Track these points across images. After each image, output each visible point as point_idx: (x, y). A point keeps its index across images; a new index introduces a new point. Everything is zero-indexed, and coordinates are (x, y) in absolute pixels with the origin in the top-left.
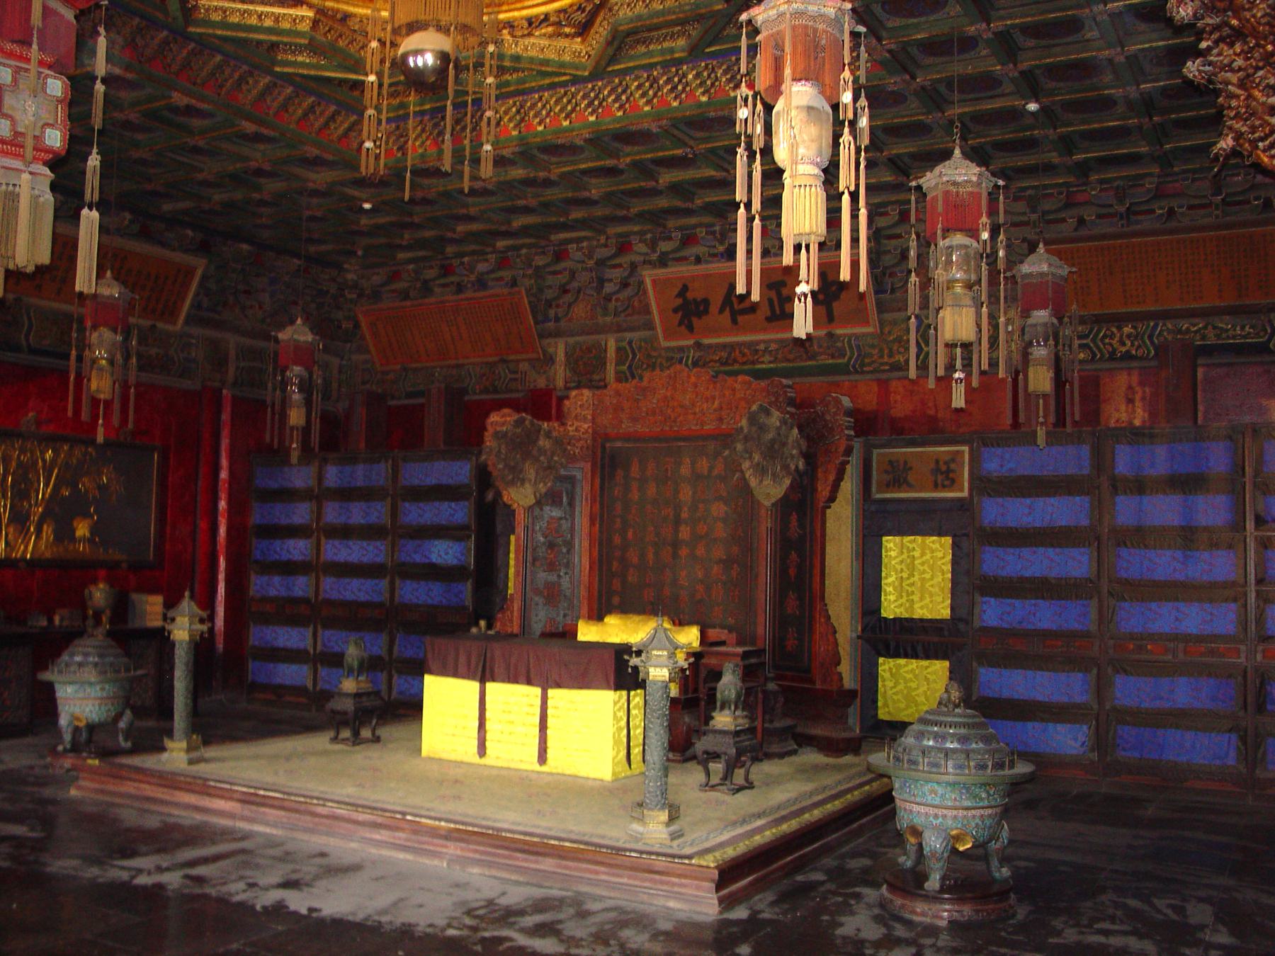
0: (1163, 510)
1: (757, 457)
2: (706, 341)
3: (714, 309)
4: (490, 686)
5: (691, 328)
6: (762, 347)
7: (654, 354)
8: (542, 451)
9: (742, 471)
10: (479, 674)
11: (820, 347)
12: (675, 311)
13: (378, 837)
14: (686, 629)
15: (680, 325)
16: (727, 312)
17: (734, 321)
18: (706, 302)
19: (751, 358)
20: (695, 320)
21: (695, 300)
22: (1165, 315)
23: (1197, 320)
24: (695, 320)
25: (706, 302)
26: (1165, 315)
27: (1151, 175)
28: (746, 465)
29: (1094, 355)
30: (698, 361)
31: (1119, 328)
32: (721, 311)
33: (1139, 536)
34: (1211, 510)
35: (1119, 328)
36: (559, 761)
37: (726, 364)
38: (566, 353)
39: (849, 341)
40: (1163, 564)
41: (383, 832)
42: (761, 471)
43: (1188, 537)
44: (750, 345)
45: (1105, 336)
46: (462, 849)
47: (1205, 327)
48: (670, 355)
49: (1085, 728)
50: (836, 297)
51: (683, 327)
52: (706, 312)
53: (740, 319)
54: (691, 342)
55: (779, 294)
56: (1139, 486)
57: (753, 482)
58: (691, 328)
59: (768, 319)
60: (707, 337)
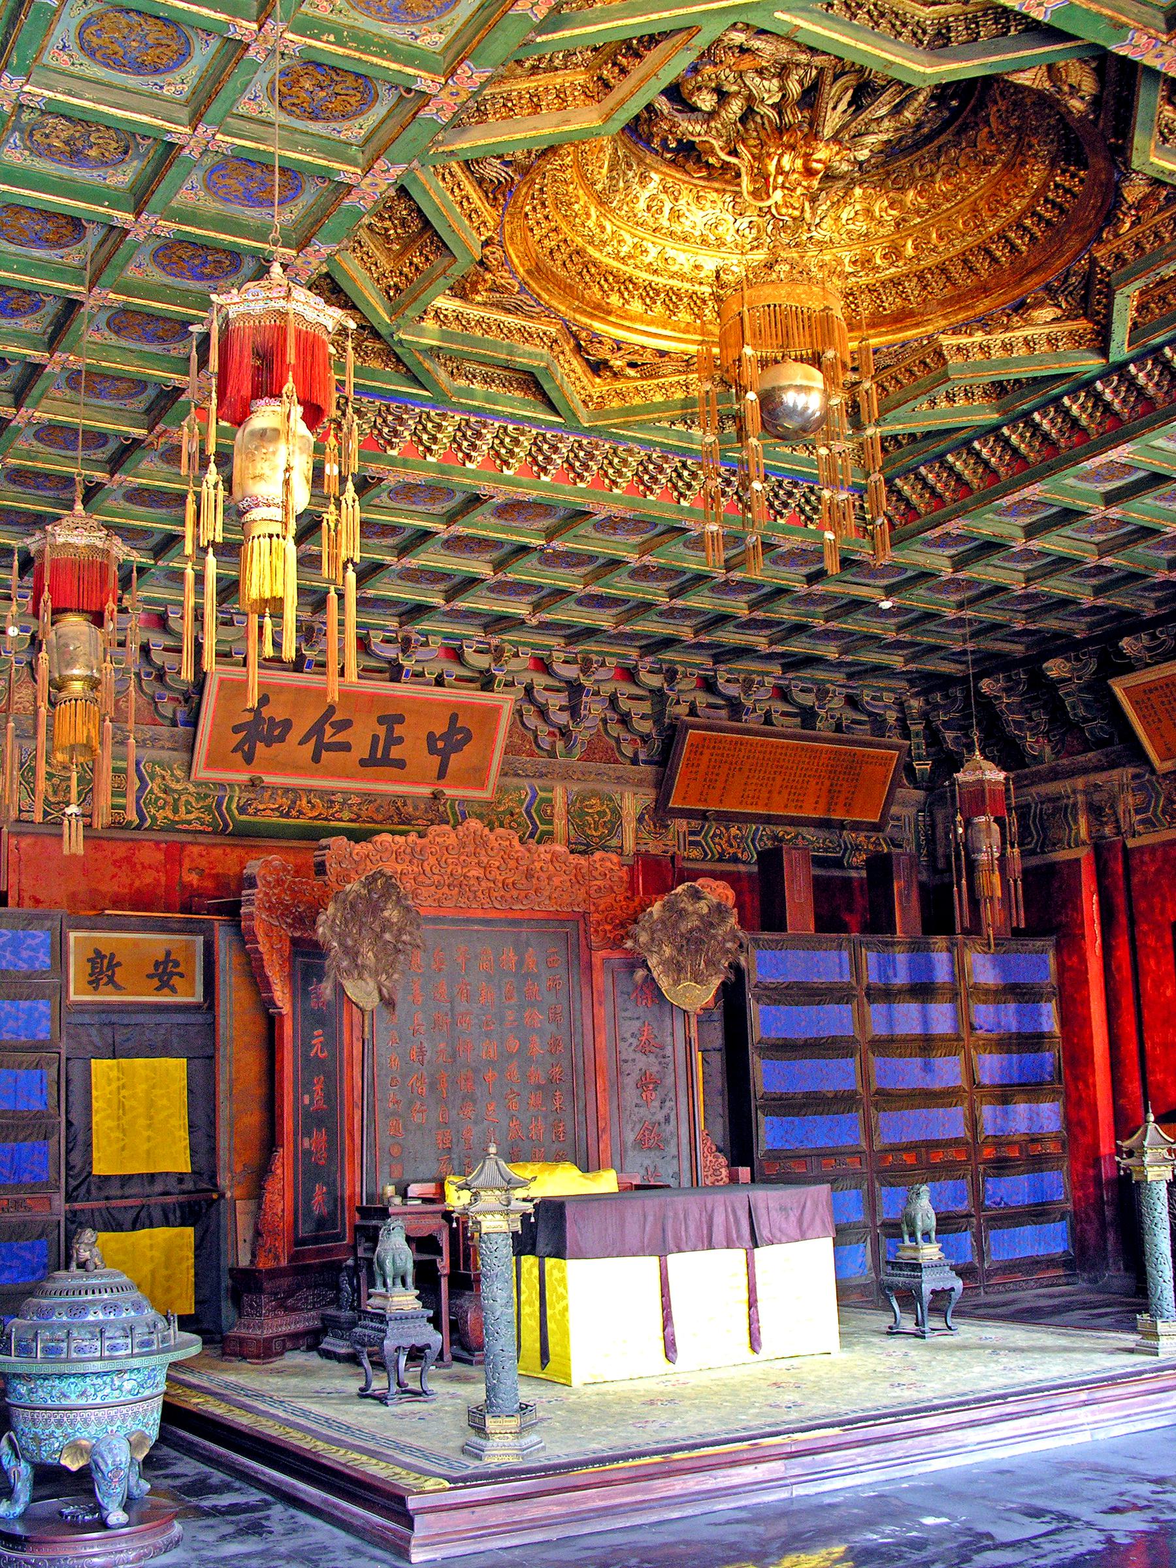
0: (907, 1018)
1: (667, 951)
2: (267, 779)
3: (294, 736)
4: (673, 1259)
5: (249, 759)
6: (339, 798)
7: (179, 787)
8: (386, 926)
9: (649, 970)
11: (416, 808)
12: (236, 729)
15: (234, 751)
16: (311, 745)
17: (316, 758)
18: (287, 725)
19: (325, 812)
20: (260, 746)
21: (272, 719)
22: (768, 820)
23: (788, 828)
24: (260, 746)
25: (287, 725)
26: (768, 820)
27: (768, 674)
28: (652, 961)
29: (706, 854)
30: (248, 803)
31: (727, 829)
33: (886, 1045)
34: (941, 1018)
35: (727, 829)
38: (22, 765)
39: (452, 807)
40: (909, 1073)
42: (676, 968)
43: (926, 1044)
44: (323, 793)
45: (715, 835)
46: (1093, 1413)
47: (796, 837)
48: (203, 790)
50: (458, 747)
51: (239, 754)
52: (281, 739)
54: (245, 777)
55: (390, 730)
56: (886, 994)
57: (664, 983)
58: (249, 759)
59: (363, 763)
60: (268, 773)
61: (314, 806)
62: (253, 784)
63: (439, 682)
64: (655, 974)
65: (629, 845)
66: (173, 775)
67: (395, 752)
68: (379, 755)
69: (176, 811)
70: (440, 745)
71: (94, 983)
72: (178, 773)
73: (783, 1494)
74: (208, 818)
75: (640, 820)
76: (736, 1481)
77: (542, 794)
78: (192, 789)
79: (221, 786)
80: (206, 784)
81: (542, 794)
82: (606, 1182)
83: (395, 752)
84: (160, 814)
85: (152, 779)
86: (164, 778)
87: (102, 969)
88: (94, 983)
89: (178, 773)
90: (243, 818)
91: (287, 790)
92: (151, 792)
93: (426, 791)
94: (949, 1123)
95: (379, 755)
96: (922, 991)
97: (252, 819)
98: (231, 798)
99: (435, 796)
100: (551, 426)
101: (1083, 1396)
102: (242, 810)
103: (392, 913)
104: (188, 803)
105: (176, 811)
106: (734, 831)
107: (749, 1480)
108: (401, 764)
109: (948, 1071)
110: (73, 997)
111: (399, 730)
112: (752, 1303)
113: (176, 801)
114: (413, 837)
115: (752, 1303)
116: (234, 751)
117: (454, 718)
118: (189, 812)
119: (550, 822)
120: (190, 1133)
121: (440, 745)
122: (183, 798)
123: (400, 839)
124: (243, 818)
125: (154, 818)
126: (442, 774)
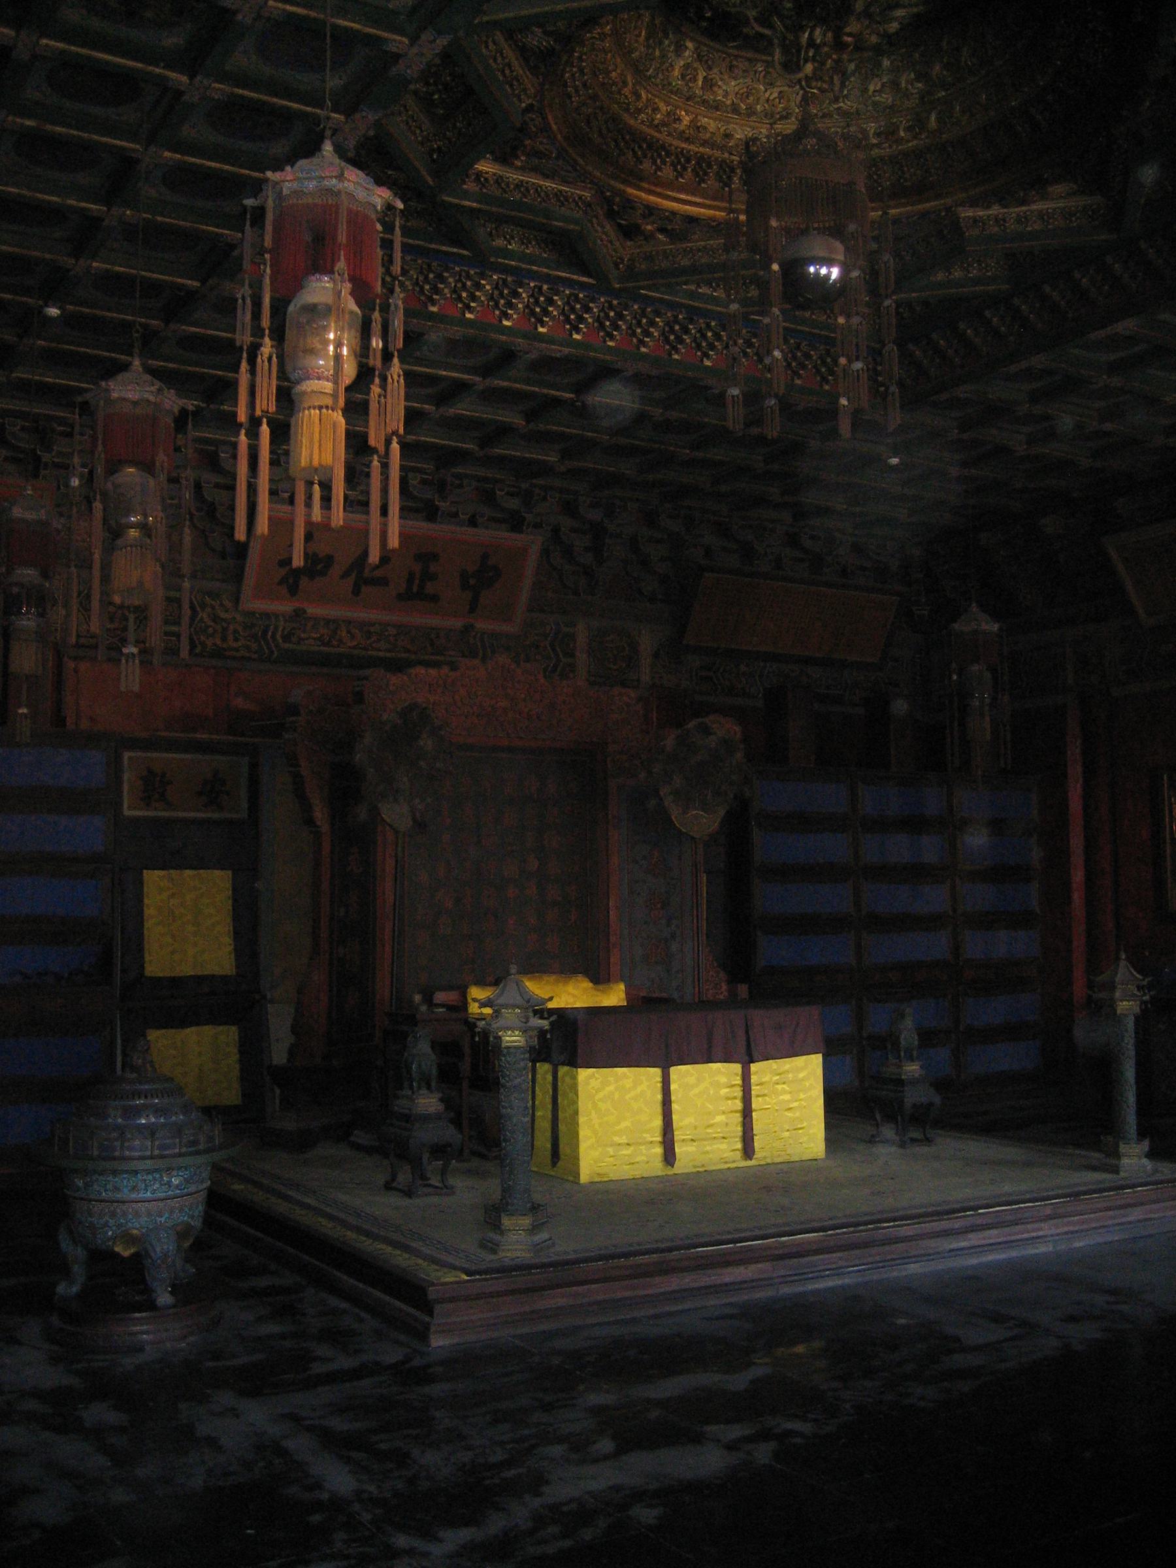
0: (898, 848)
2: (311, 610)
3: (336, 570)
4: (676, 1072)
5: (293, 590)
10: (743, 1050)
13: (963, 1244)
14: (614, 986)
15: (280, 583)
16: (351, 579)
17: (356, 591)
28: (664, 791)
32: (345, 575)
36: (767, 1149)
37: (328, 644)
41: (970, 1236)
43: (917, 873)
49: (848, 1058)
53: (364, 589)
54: (285, 607)
57: (675, 813)
58: (293, 590)
59: (400, 597)
61: (353, 637)
62: (298, 614)
63: (472, 522)
64: (666, 804)
65: (646, 678)
66: (222, 605)
67: (430, 588)
68: (415, 589)
69: (224, 639)
70: (472, 582)
71: (147, 799)
72: (227, 603)
73: (769, 1293)
74: (254, 646)
75: (656, 655)
76: (727, 1280)
77: (566, 630)
78: (239, 618)
79: (267, 615)
80: (253, 613)
81: (566, 630)
82: (615, 997)
83: (430, 588)
84: (209, 642)
85: (203, 609)
86: (213, 608)
87: (154, 786)
88: (147, 799)
89: (227, 603)
90: (287, 646)
91: (328, 622)
92: (202, 619)
93: (458, 624)
94: (932, 946)
95: (415, 589)
96: (914, 824)
97: (295, 646)
98: (276, 628)
99: (467, 629)
100: (583, 286)
101: (1048, 1211)
102: (286, 638)
103: (427, 743)
104: (235, 631)
105: (224, 639)
106: (743, 668)
107: (739, 1279)
108: (434, 598)
109: (933, 898)
110: (127, 812)
111: (433, 568)
112: (747, 1112)
113: (225, 629)
114: (445, 669)
115: (747, 1112)
116: (280, 583)
117: (485, 557)
118: (236, 640)
119: (572, 656)
120: (235, 939)
121: (472, 582)
122: (231, 627)
123: (433, 672)
124: (287, 646)
125: (203, 644)
126: (472, 610)
